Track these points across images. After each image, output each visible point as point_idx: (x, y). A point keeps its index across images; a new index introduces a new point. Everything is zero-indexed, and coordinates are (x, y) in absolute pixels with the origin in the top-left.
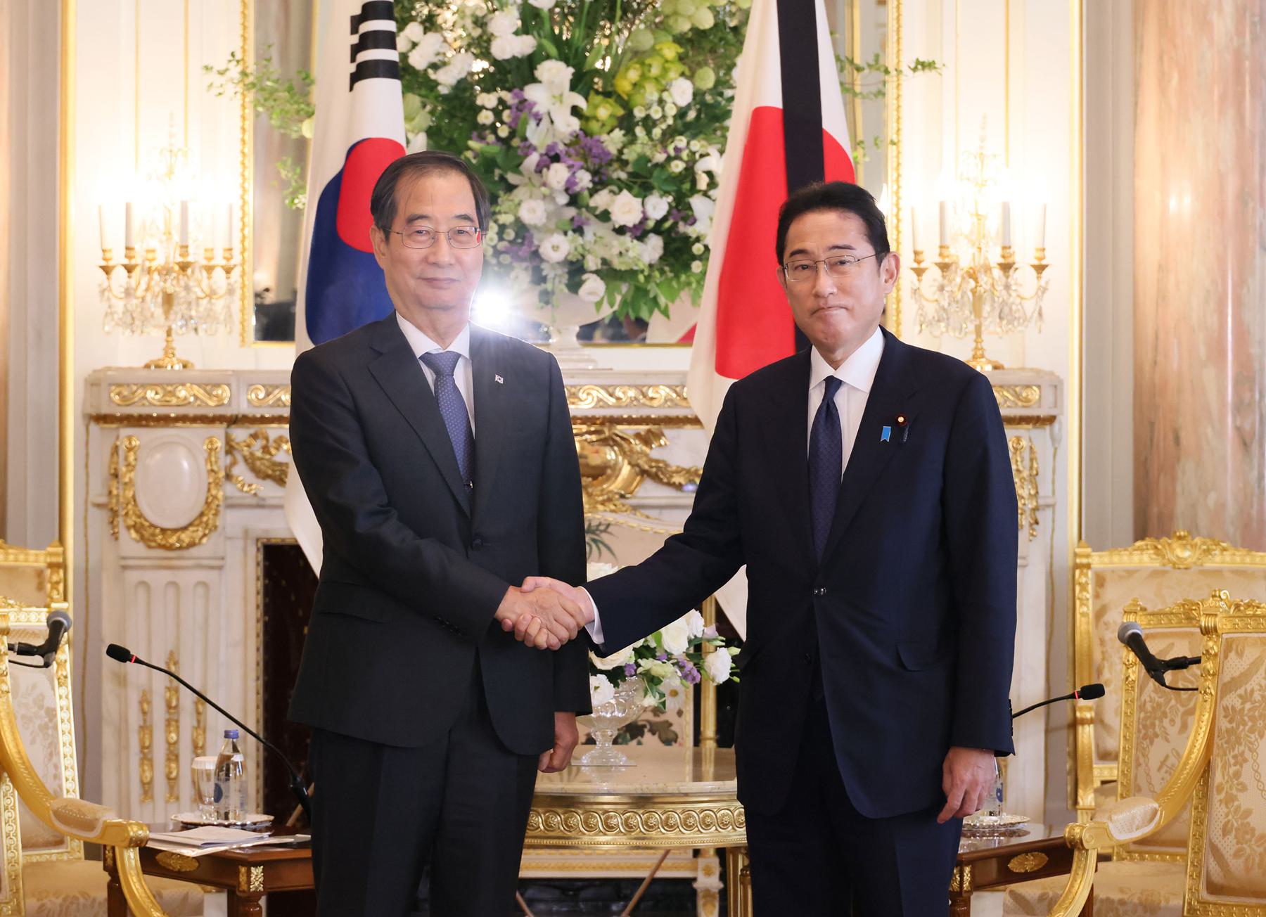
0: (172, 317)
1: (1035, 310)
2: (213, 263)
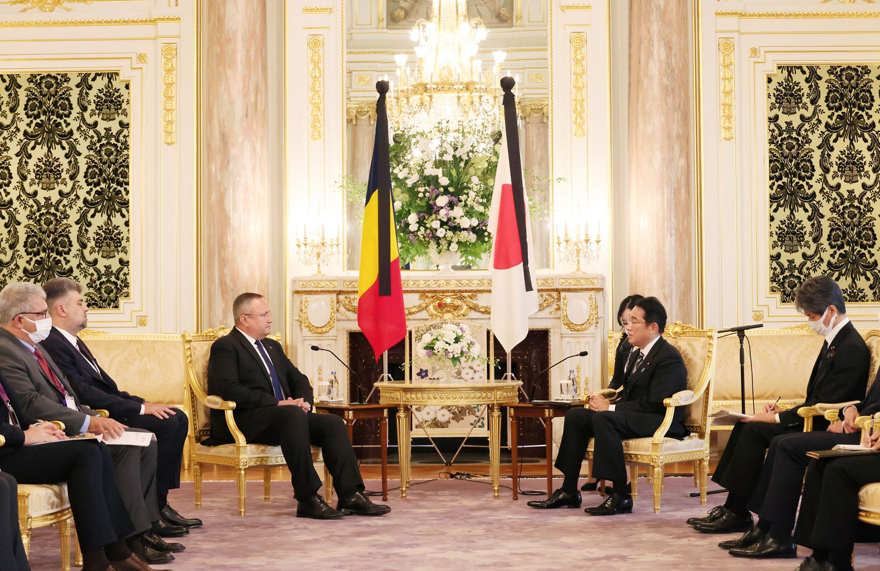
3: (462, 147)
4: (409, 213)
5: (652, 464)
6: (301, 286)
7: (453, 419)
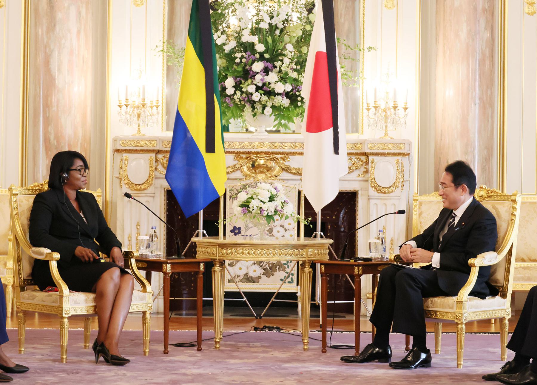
0: (140, 120)
1: (403, 122)
2: (153, 105)
3: (278, 15)
4: (226, 77)
5: (456, 321)
6: (122, 145)
7: (264, 274)
